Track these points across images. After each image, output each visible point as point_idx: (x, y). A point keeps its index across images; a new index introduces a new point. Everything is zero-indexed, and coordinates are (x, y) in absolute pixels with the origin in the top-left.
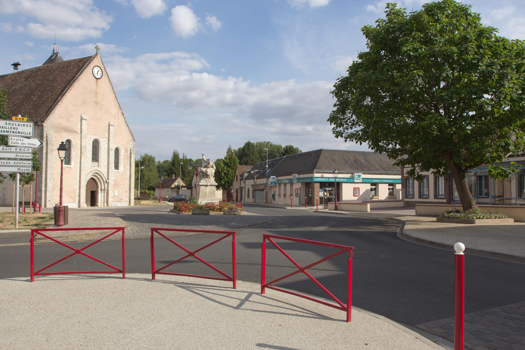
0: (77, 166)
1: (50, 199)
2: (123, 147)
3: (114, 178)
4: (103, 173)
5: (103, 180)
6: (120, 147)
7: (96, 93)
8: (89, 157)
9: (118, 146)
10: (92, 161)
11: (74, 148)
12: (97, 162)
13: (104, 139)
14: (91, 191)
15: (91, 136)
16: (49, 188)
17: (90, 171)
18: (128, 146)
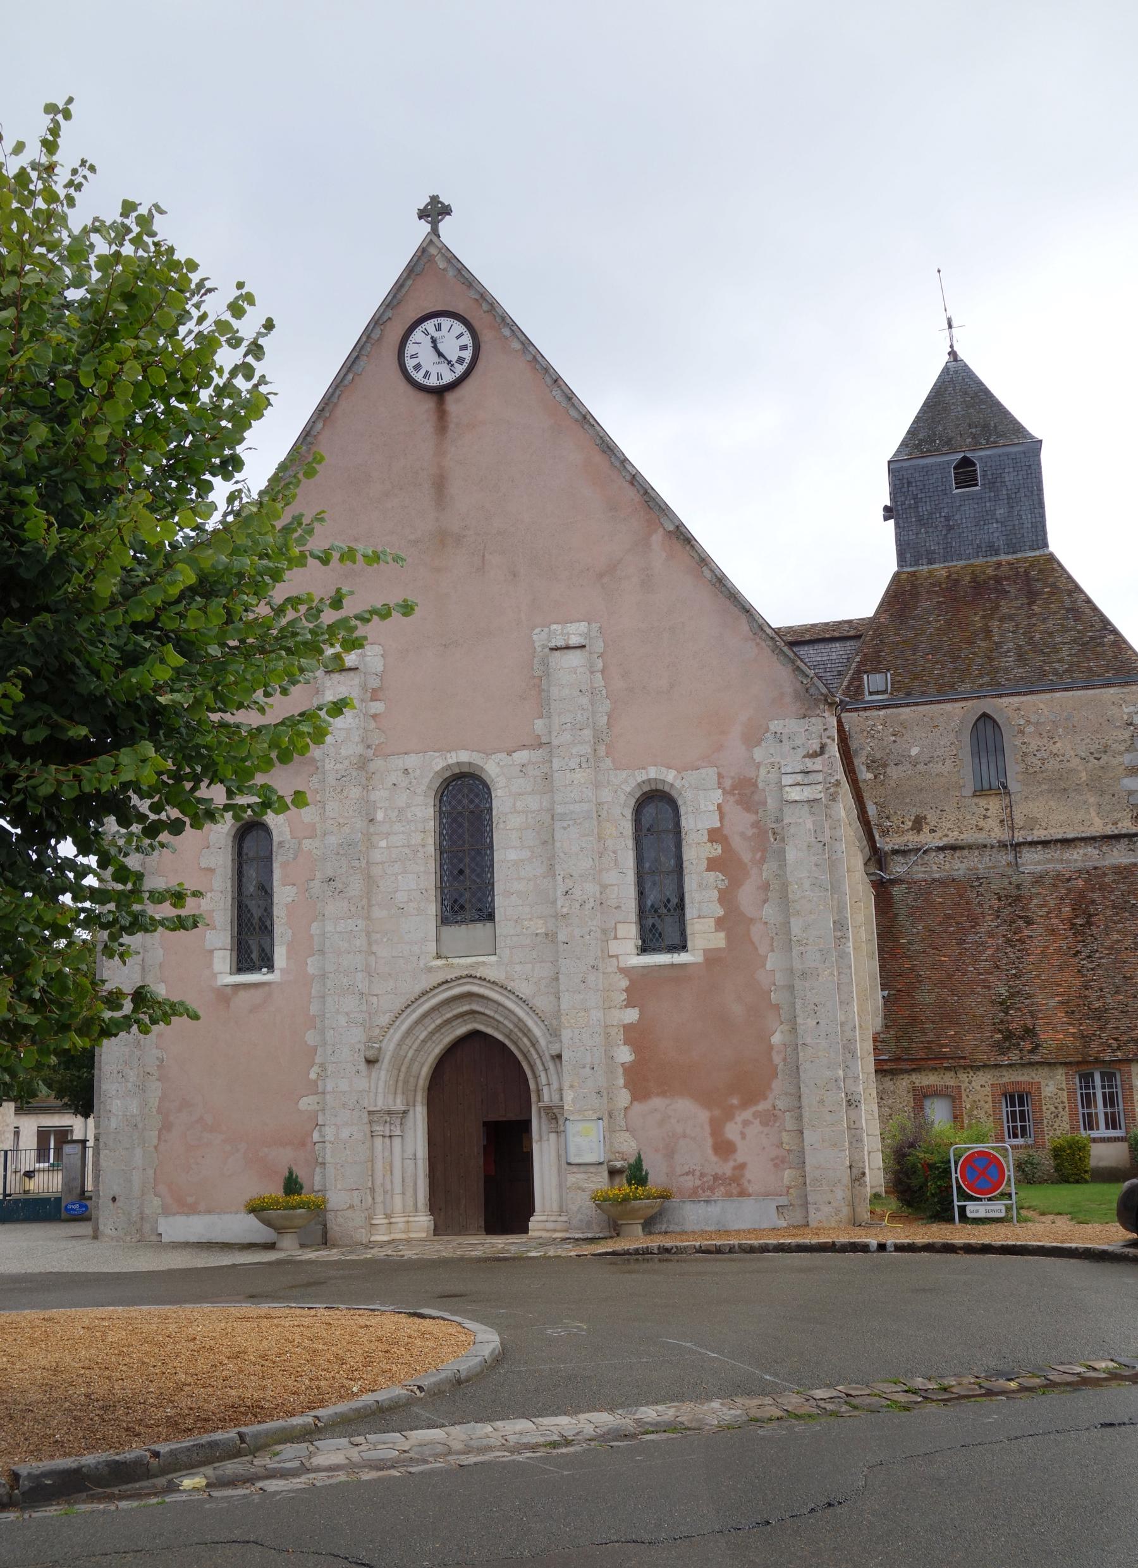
0: (311, 970)
1: (116, 1190)
2: (710, 774)
3: (632, 1015)
4: (524, 989)
5: (534, 1043)
6: (670, 776)
7: (440, 484)
8: (401, 897)
9: (652, 773)
10: (444, 920)
11: (284, 865)
12: (489, 925)
13: (522, 756)
14: (486, 1124)
15: (412, 761)
16: (114, 1123)
17: (418, 989)
18: (758, 754)
